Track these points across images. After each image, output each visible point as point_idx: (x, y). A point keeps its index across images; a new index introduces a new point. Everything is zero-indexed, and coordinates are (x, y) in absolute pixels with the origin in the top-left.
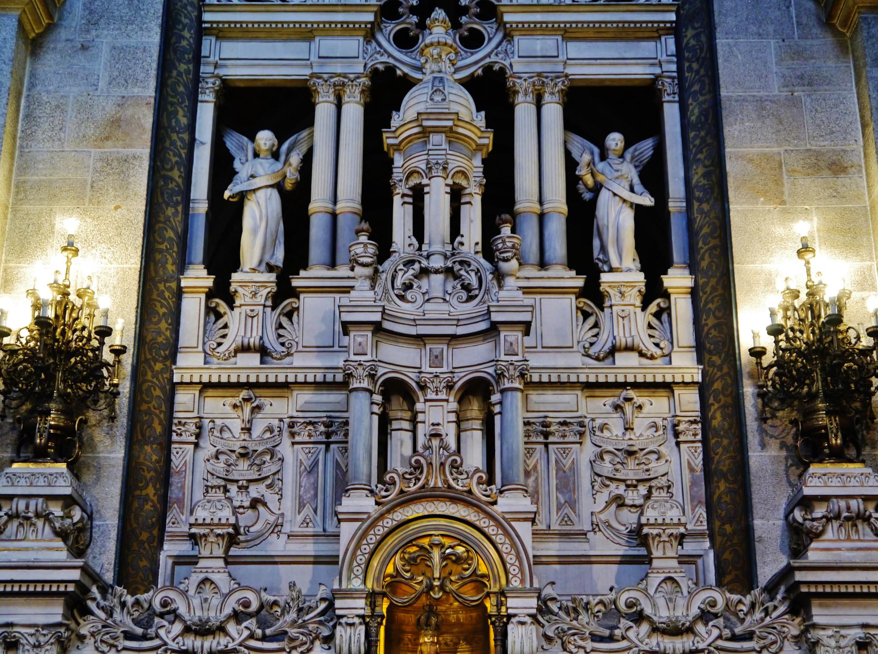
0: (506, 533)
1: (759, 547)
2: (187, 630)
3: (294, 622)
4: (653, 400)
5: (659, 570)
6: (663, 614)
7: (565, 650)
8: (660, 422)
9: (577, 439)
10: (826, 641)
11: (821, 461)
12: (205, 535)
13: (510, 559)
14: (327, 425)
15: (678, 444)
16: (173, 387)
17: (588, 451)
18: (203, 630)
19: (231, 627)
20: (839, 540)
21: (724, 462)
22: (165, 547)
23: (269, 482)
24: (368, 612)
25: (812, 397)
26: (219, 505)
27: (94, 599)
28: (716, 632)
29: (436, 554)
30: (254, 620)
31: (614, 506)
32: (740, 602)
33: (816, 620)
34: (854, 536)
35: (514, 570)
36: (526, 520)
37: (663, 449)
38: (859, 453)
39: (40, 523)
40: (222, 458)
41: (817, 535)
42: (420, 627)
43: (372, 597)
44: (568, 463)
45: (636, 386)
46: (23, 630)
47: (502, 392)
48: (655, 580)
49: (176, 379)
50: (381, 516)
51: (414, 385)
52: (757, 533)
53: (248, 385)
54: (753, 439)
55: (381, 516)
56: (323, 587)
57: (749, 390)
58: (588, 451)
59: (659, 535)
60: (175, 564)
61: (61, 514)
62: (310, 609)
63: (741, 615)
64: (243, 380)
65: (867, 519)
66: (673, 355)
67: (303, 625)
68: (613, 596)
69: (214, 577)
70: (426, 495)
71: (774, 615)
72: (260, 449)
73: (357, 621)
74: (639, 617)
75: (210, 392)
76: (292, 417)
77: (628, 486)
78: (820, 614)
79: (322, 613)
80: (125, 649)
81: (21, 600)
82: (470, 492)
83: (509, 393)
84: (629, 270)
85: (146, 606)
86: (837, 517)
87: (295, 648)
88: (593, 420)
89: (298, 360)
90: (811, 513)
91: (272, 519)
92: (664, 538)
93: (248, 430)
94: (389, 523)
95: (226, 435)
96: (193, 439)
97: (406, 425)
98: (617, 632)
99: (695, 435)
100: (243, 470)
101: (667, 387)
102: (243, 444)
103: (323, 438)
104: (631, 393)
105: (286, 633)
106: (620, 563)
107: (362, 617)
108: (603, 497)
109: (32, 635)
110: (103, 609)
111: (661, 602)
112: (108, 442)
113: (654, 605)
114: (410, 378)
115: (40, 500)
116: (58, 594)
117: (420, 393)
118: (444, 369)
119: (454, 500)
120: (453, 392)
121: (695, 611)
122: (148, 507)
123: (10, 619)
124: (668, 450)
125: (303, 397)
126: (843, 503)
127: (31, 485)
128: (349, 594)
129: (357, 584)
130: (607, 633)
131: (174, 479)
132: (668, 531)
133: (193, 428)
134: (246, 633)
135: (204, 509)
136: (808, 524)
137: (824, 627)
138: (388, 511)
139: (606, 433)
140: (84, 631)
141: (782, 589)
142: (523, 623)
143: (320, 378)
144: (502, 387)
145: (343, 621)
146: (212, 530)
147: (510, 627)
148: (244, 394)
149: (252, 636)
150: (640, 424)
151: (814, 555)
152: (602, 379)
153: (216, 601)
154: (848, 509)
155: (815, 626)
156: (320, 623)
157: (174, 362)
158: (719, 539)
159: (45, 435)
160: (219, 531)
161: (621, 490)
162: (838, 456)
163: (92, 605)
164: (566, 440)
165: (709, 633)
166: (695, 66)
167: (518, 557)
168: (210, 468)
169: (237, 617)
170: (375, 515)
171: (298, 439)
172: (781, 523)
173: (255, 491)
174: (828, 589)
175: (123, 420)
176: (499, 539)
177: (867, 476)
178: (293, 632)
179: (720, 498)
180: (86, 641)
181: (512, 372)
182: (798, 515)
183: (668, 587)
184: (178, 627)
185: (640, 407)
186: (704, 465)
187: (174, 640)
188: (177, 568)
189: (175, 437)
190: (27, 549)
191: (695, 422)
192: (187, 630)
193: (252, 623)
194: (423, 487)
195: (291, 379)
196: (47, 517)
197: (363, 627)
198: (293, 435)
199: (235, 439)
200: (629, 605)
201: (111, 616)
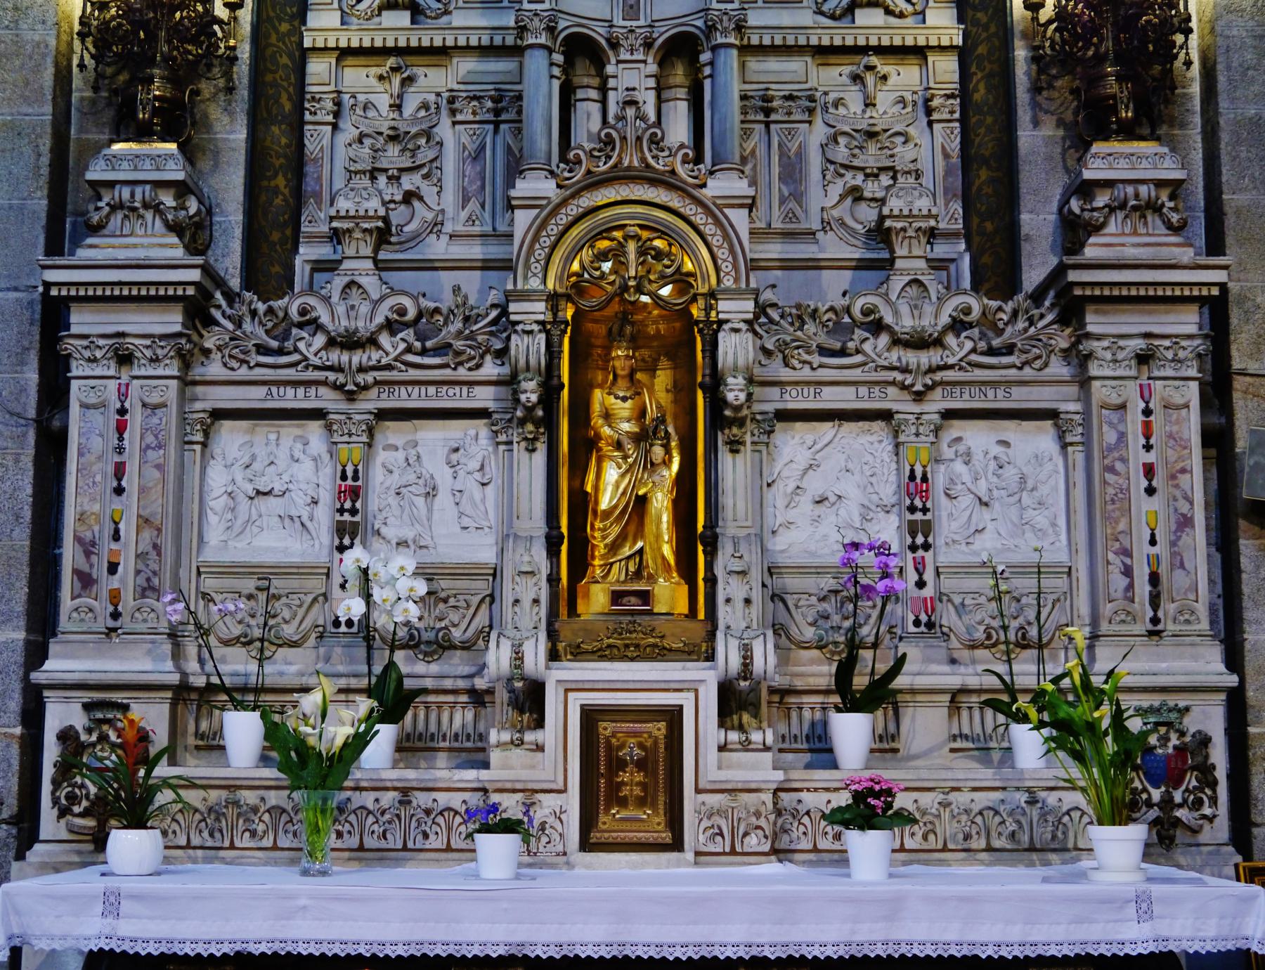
0: (717, 222)
1: (1026, 248)
2: (331, 343)
3: (460, 332)
4: (900, 69)
5: (902, 272)
6: (906, 323)
7: (787, 365)
8: (909, 97)
9: (806, 117)
10: (1100, 353)
11: (1106, 139)
12: (349, 231)
13: (722, 254)
14: (496, 100)
15: (930, 124)
16: (303, 55)
17: (819, 132)
18: (350, 342)
19: (384, 339)
20: (1123, 234)
21: (986, 143)
22: (301, 250)
23: (425, 171)
24: (549, 317)
25: (1100, 59)
26: (364, 194)
27: (219, 307)
28: (969, 345)
29: (632, 247)
30: (411, 331)
31: (849, 200)
32: (1000, 309)
33: (1090, 328)
34: (1142, 230)
35: (726, 267)
36: (741, 206)
37: (911, 130)
38: (1153, 132)
39: (149, 215)
40: (367, 142)
41: (1098, 228)
42: (613, 338)
43: (553, 300)
44: (794, 147)
45: (880, 50)
46: (137, 342)
47: (714, 49)
48: (898, 282)
49: (307, 43)
50: (564, 202)
51: (603, 42)
52: (1025, 230)
53: (396, 51)
54: (1024, 115)
55: (564, 202)
56: (494, 292)
57: (1021, 53)
58: (819, 132)
59: (904, 229)
60: (313, 270)
61: (174, 204)
63: (1000, 324)
64: (390, 43)
65: (1157, 209)
66: (928, 12)
67: (472, 337)
68: (845, 302)
69: (363, 280)
70: (619, 176)
71: (1040, 325)
72: (414, 130)
73: (536, 327)
74: (877, 327)
75: (350, 61)
76: (452, 90)
77: (867, 176)
78: (1095, 322)
79: (495, 322)
80: (258, 365)
81: (133, 306)
82: (673, 172)
83: (722, 51)
85: (281, 314)
86: (1123, 206)
87: (461, 363)
88: (826, 93)
89: (458, 19)
90: (1091, 203)
91: (430, 216)
92: (911, 233)
93: (398, 107)
94: (573, 210)
95: (371, 113)
96: (330, 118)
97: (593, 94)
98: (851, 345)
99: (952, 112)
100: (393, 156)
101: (919, 53)
102: (393, 123)
103: (490, 117)
104: (874, 60)
105: (450, 345)
106: (856, 268)
107: (542, 323)
108: (836, 189)
110: (229, 318)
111: (904, 309)
112: (226, 120)
113: (896, 313)
114: (599, 33)
115: (148, 187)
116: (175, 299)
117: (610, 53)
118: (642, 22)
119: (655, 182)
120: (652, 52)
121: (945, 319)
122: (278, 201)
123: (121, 328)
124: (917, 131)
125: (465, 66)
126: (1130, 190)
127: (136, 169)
128: (525, 296)
129: (535, 283)
130: (838, 345)
131: (309, 169)
133: (329, 105)
134: (402, 346)
135: (347, 198)
136: (1087, 215)
137: (1099, 337)
138: (573, 196)
139: (842, 110)
140: (208, 344)
141: (1052, 293)
142: (736, 331)
143: (485, 41)
144: (714, 43)
145: (519, 328)
146: (357, 224)
147: (721, 335)
148: (392, 61)
149: (409, 350)
150: (884, 99)
151: (1091, 252)
152: (838, 42)
153: (364, 308)
154: (1137, 196)
155: (1088, 336)
156: (491, 333)
157: (304, 22)
158: (976, 239)
159: (149, 108)
160: (366, 226)
161: (859, 179)
162: (1129, 132)
163: (217, 314)
164: (793, 118)
165: (961, 346)
167: (732, 251)
169: (391, 327)
170: (556, 200)
171: (459, 117)
172: (1053, 217)
173: (408, 182)
174: (1107, 292)
175: (243, 93)
176: (709, 229)
177: (1162, 157)
178: (458, 344)
179: (980, 189)
180: (212, 356)
181: (726, 24)
182: (1075, 205)
183: (913, 291)
185: (884, 78)
186: (961, 149)
187: (316, 355)
188: (316, 275)
189: (308, 117)
190: (135, 246)
191: (952, 96)
192: (331, 343)
193: (409, 334)
194: (615, 166)
195: (450, 42)
196: (157, 208)
197: (543, 336)
198: (453, 112)
199: (383, 118)
200: (866, 312)
201: (240, 326)
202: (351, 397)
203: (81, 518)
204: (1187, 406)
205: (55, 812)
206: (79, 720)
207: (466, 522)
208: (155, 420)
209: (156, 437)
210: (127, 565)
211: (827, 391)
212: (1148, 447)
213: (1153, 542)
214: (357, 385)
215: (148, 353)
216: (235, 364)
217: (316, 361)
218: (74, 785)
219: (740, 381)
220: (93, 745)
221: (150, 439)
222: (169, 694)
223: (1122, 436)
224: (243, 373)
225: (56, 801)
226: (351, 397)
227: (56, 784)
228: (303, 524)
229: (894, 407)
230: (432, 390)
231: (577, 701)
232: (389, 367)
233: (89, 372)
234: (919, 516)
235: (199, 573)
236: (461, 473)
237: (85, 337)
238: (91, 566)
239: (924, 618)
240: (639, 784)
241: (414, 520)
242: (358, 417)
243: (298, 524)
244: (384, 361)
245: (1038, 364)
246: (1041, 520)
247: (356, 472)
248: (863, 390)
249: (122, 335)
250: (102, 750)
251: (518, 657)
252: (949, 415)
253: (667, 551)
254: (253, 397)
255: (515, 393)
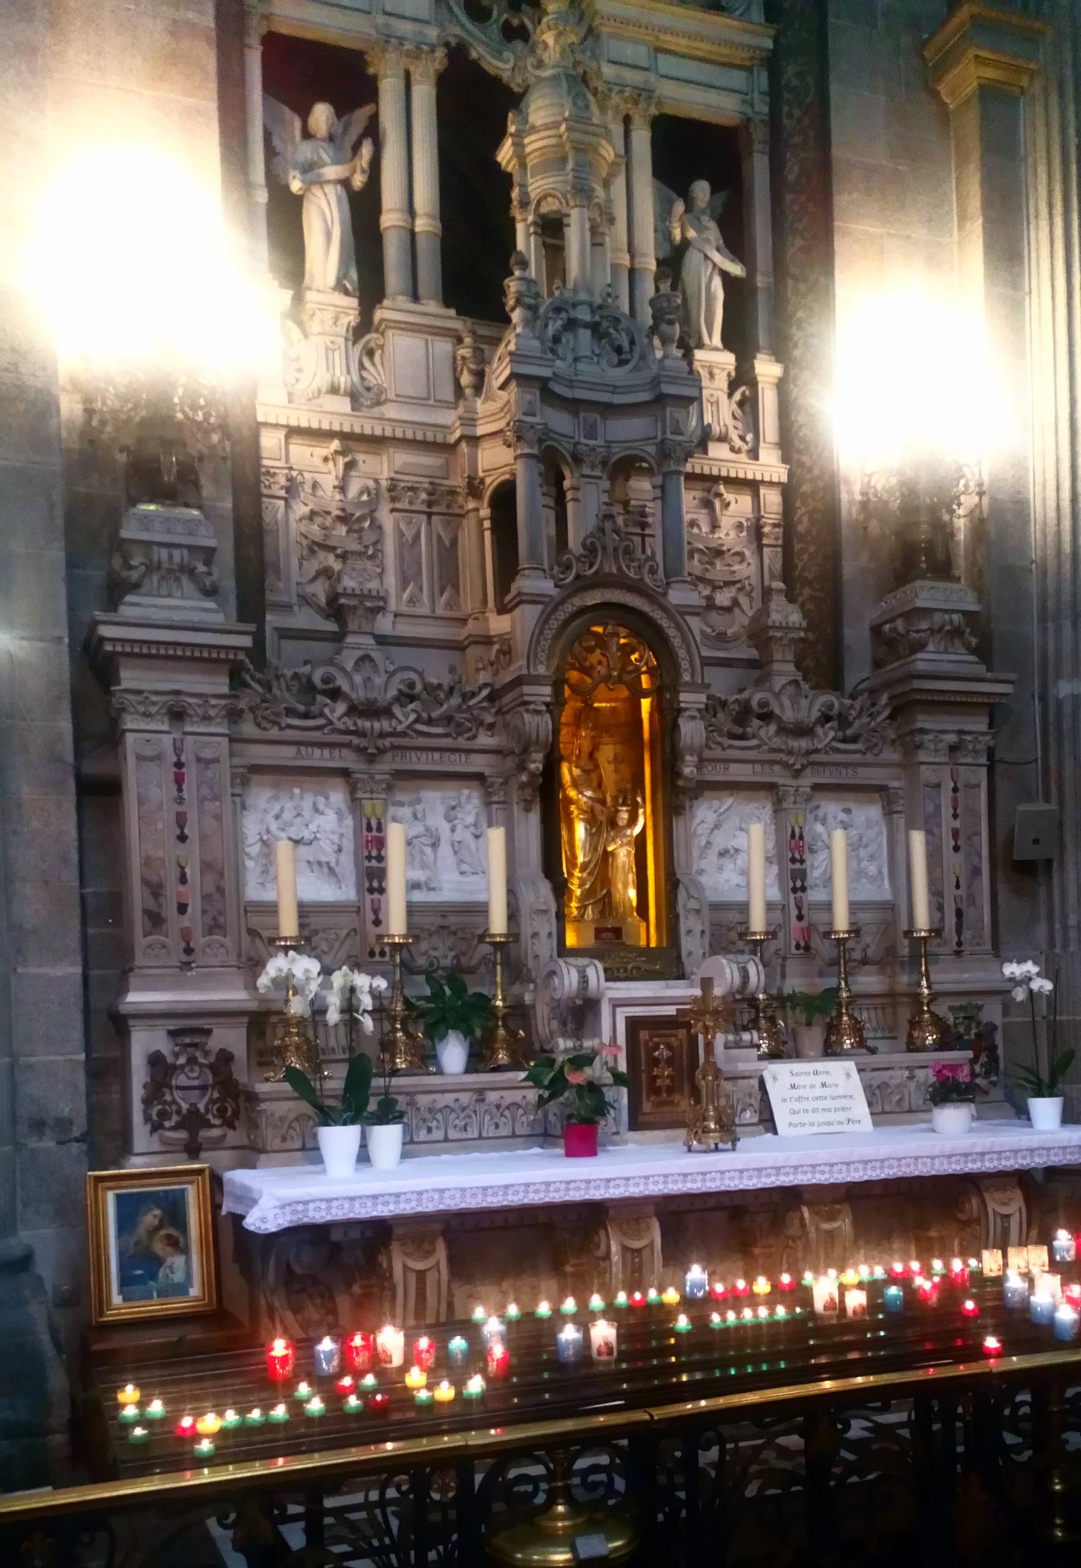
2: (353, 710)
3: (460, 706)
5: (781, 674)
6: (788, 715)
14: (430, 494)
28: (832, 734)
48: (779, 682)
59: (781, 639)
62: (473, 695)
69: (373, 654)
72: (358, 514)
74: (767, 717)
84: (717, 349)
89: (391, 411)
92: (786, 642)
96: (282, 493)
98: (749, 730)
103: (424, 508)
109: (140, 703)
110: (259, 682)
111: (787, 702)
132: (791, 635)
134: (412, 717)
142: (693, 718)
147: (681, 721)
153: (379, 680)
163: (247, 678)
165: (826, 734)
166: (797, 113)
168: (303, 529)
178: (459, 717)
180: (245, 716)
184: (341, 708)
187: (339, 719)
198: (393, 499)
199: (330, 498)
201: (270, 690)
202: (371, 759)
203: (147, 861)
204: (978, 786)
205: (148, 1127)
206: (163, 1045)
207: (465, 867)
208: (209, 774)
209: (211, 789)
210: (195, 906)
211: (733, 767)
212: (955, 816)
213: (958, 887)
214: (378, 748)
215: (200, 711)
216: (265, 724)
217: (340, 725)
218: (165, 1103)
219: (695, 758)
220: (183, 1066)
221: (205, 791)
222: (246, 1020)
223: (938, 807)
224: (274, 733)
225: (147, 1118)
226: (371, 759)
227: (147, 1102)
228: (331, 869)
229: (780, 781)
230: (437, 755)
231: (622, 1014)
232: (403, 734)
233: (143, 726)
234: (798, 866)
235: (246, 912)
236: (459, 828)
237: (139, 692)
238: (160, 906)
239: (802, 943)
240: (668, 1077)
241: (424, 866)
242: (378, 777)
243: (325, 870)
244: (399, 728)
245: (875, 751)
246: (872, 869)
247: (379, 825)
248: (758, 767)
249: (178, 693)
250: (192, 1071)
251: (584, 979)
252: (816, 787)
253: (632, 893)
254: (285, 755)
255: (524, 761)
